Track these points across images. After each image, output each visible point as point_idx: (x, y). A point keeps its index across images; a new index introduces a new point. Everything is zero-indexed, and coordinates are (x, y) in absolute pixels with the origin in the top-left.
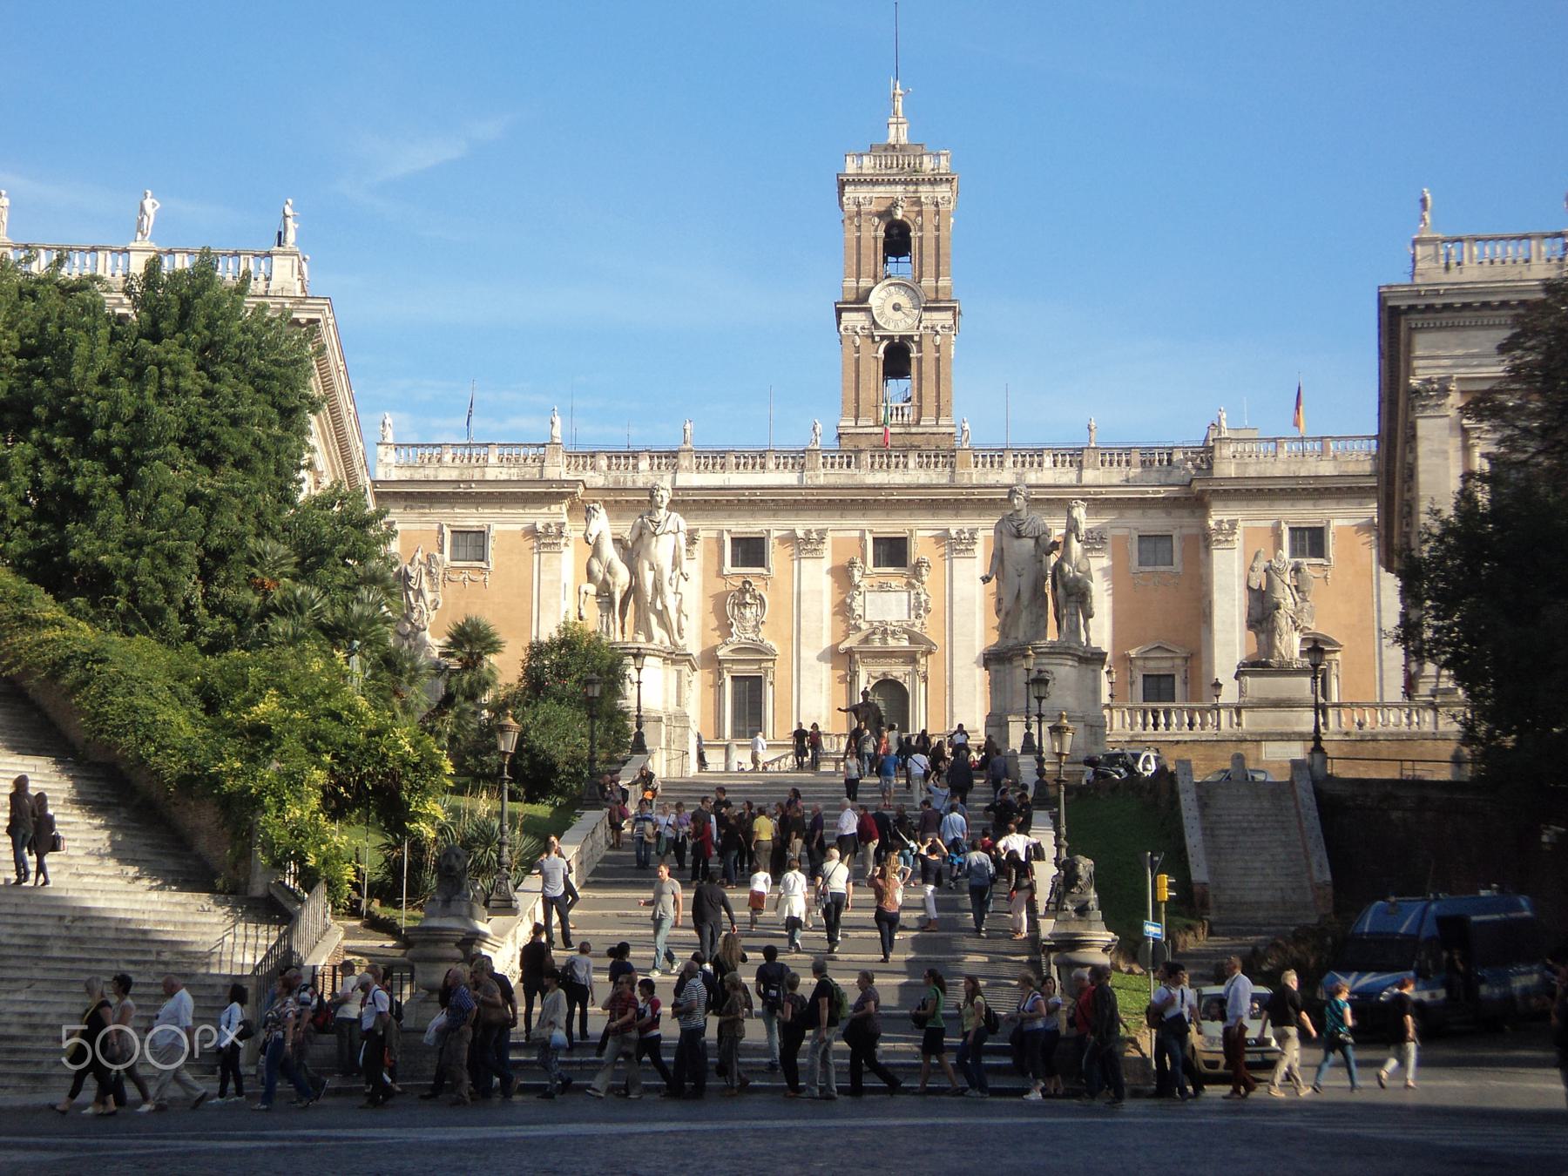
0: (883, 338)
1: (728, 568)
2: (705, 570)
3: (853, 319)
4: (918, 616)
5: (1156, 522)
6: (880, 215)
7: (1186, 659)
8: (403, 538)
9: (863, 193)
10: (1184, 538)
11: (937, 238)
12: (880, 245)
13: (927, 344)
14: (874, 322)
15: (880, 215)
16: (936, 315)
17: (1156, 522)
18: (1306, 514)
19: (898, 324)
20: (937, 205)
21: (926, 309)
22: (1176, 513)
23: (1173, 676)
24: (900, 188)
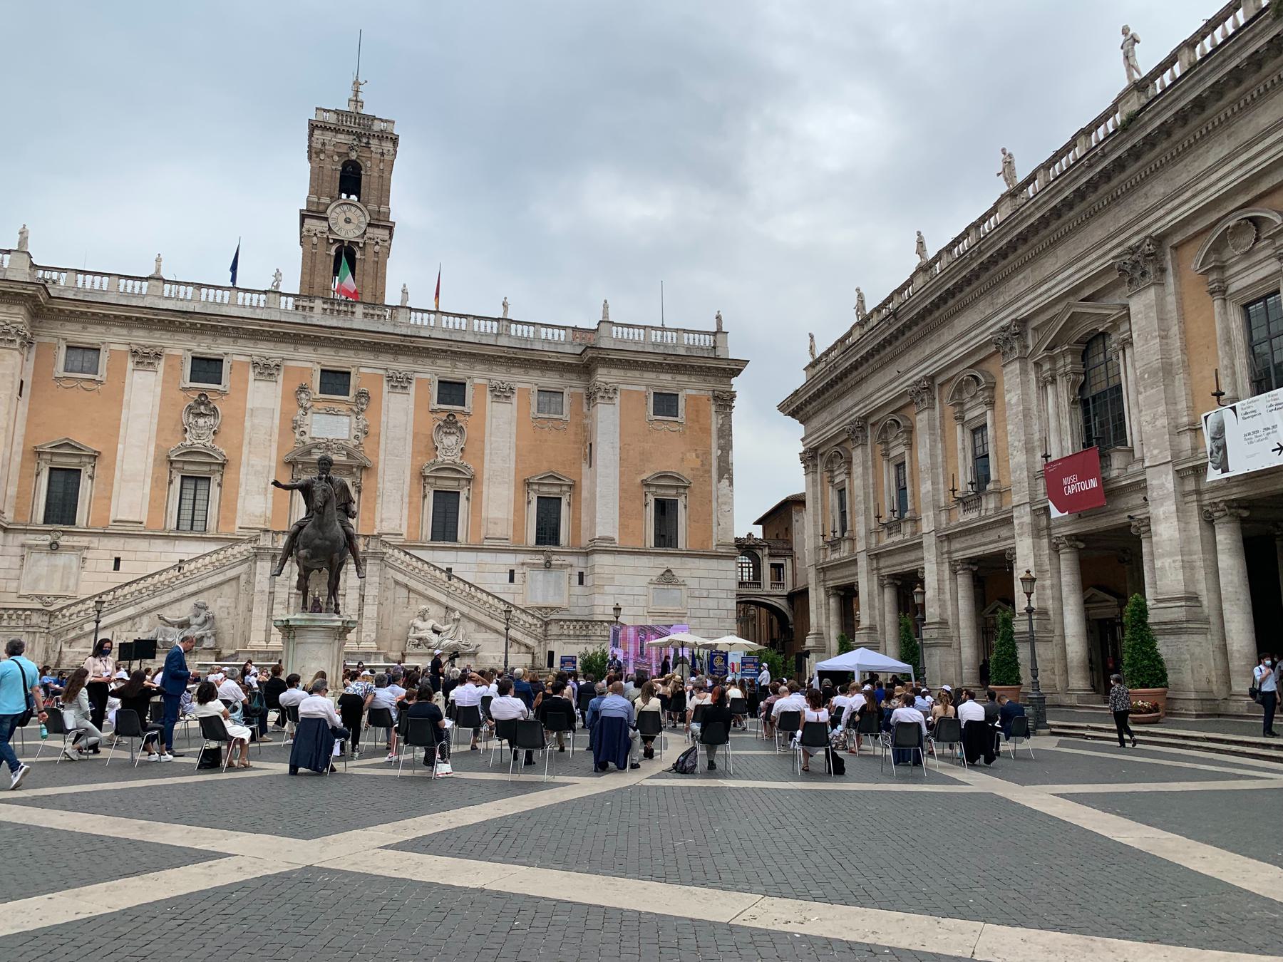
2: (164, 381)
4: (357, 437)
5: (551, 381)
7: (570, 486)
9: (328, 136)
12: (338, 176)
13: (368, 247)
14: (330, 229)
16: (376, 231)
18: (666, 381)
20: (382, 154)
21: (370, 225)
22: (568, 376)
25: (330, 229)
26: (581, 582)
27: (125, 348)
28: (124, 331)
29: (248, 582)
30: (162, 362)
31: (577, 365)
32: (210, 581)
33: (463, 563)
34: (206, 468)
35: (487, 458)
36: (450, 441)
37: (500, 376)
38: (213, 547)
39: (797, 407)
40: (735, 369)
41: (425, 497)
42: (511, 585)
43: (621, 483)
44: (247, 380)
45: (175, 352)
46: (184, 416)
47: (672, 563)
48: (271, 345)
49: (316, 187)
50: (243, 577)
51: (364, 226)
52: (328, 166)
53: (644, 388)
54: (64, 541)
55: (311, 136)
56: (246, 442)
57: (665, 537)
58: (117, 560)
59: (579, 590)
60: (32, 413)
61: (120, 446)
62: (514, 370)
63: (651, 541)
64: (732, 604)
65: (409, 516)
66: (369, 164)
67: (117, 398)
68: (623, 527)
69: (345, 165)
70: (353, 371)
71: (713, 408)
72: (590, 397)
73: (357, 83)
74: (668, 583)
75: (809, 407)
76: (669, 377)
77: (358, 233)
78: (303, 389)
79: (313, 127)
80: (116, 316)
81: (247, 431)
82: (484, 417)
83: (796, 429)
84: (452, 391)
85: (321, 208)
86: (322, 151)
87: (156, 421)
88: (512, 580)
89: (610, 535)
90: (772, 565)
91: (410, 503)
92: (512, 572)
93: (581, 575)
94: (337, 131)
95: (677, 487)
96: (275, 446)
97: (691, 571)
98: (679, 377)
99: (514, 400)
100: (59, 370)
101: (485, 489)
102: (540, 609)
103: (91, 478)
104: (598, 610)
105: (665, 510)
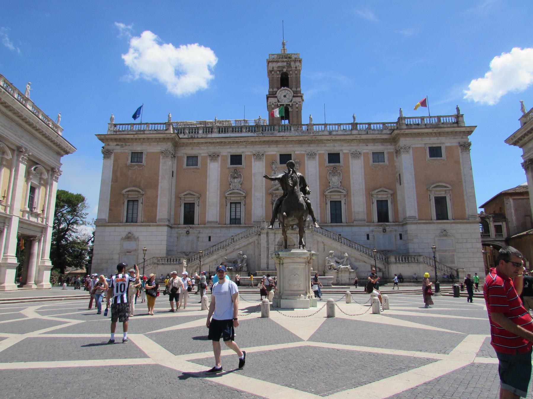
0: (281, 105)
1: (229, 165)
2: (221, 166)
3: (272, 100)
5: (378, 148)
6: (280, 71)
7: (392, 195)
8: (115, 155)
9: (275, 65)
10: (388, 153)
11: (296, 77)
13: (294, 107)
14: (278, 101)
15: (280, 71)
17: (378, 148)
19: (285, 101)
20: (296, 68)
21: (294, 96)
22: (385, 144)
23: (387, 201)
24: (285, 64)
25: (278, 101)
26: (401, 238)
27: (207, 155)
28: (206, 148)
29: (258, 243)
30: (220, 158)
31: (390, 139)
32: (244, 244)
33: (346, 231)
34: (239, 199)
35: (352, 185)
36: (335, 180)
37: (354, 147)
38: (244, 230)
39: (515, 140)
40: (469, 131)
41: (326, 204)
42: (368, 241)
43: (417, 191)
44: (251, 162)
45: (225, 154)
46: (229, 179)
47: (447, 227)
48: (260, 146)
49: (271, 86)
50: (256, 242)
51: (291, 98)
52: (275, 76)
53: (423, 146)
54: (191, 231)
55: (268, 65)
56: (253, 186)
57: (442, 215)
58: (210, 237)
59: (399, 242)
60: (177, 182)
61: (207, 193)
62: (360, 144)
63: (434, 216)
64: (480, 245)
65: (321, 213)
66: (291, 72)
67: (205, 174)
68: (420, 211)
69: (282, 75)
70: (292, 153)
71: (460, 151)
72: (398, 152)
73: (283, 44)
74: (446, 236)
75: (526, 138)
76: (436, 138)
77: (289, 101)
78: (273, 163)
79: (269, 62)
80: (202, 143)
81: (253, 182)
82: (349, 167)
83: (517, 152)
84: (334, 158)
85: (274, 93)
86: (272, 71)
87: (219, 181)
88: (368, 238)
89: (414, 215)
90: (495, 226)
91: (320, 207)
92: (368, 235)
93: (401, 235)
94: (277, 62)
95: (445, 191)
96: (264, 187)
97: (459, 230)
98: (440, 138)
99: (362, 158)
100: (185, 166)
101: (352, 198)
102: (382, 251)
103: (198, 206)
104: (411, 251)
105: (440, 202)
